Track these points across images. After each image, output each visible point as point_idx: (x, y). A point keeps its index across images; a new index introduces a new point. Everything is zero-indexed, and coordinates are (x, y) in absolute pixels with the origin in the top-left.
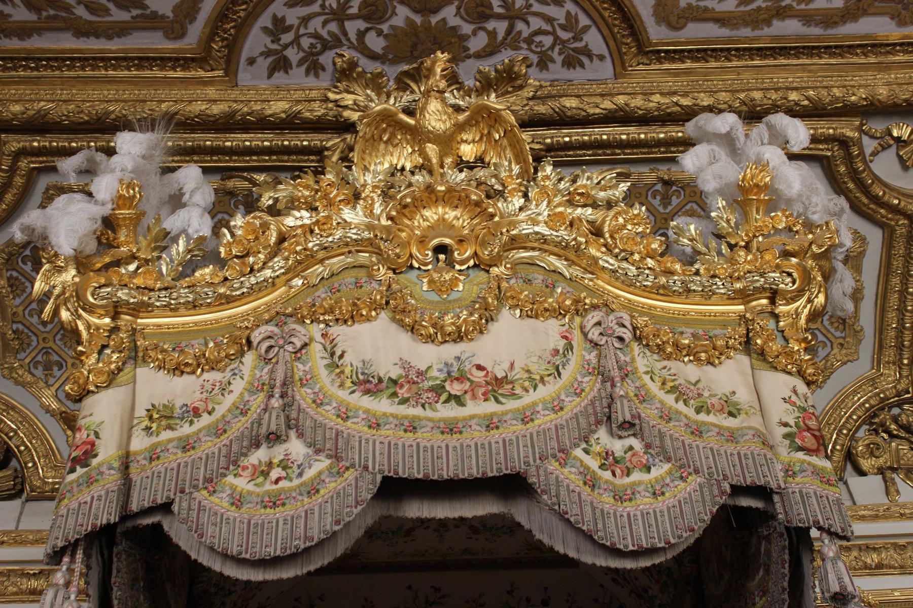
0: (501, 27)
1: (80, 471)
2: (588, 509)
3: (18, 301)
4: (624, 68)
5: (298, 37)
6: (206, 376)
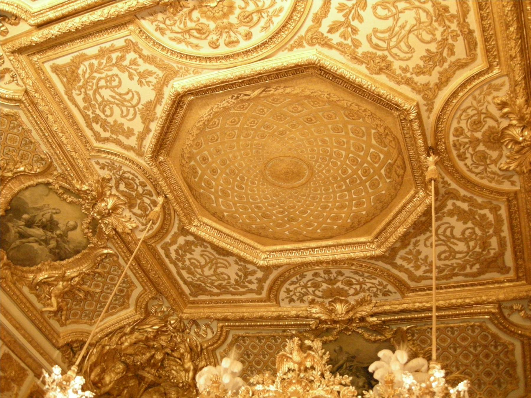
0: (358, 287)
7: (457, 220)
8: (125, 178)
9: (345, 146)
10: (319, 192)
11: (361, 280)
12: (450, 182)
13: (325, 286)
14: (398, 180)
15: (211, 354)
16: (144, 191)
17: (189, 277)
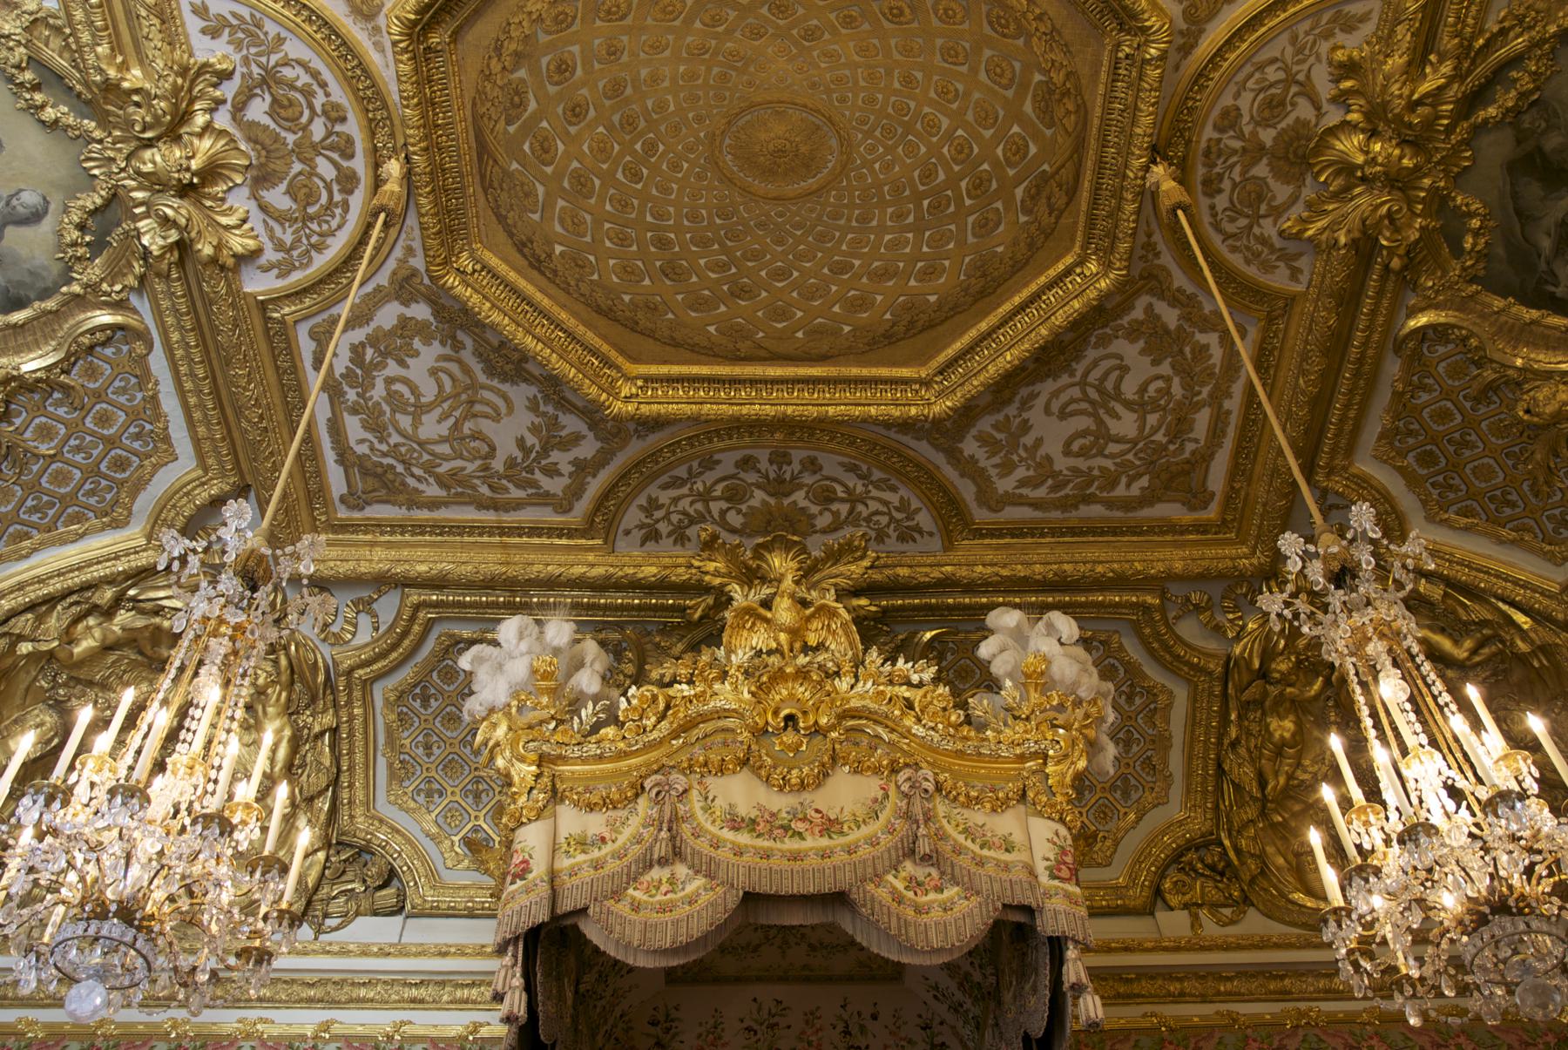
0: (844, 509)
1: (519, 883)
2: (894, 920)
3: (406, 734)
4: (951, 542)
5: (669, 513)
7: (1143, 352)
8: (279, 82)
9: (955, 106)
10: (842, 222)
11: (860, 489)
12: (1161, 247)
13: (759, 497)
14: (1047, 220)
15: (357, 694)
16: (329, 134)
17: (362, 441)
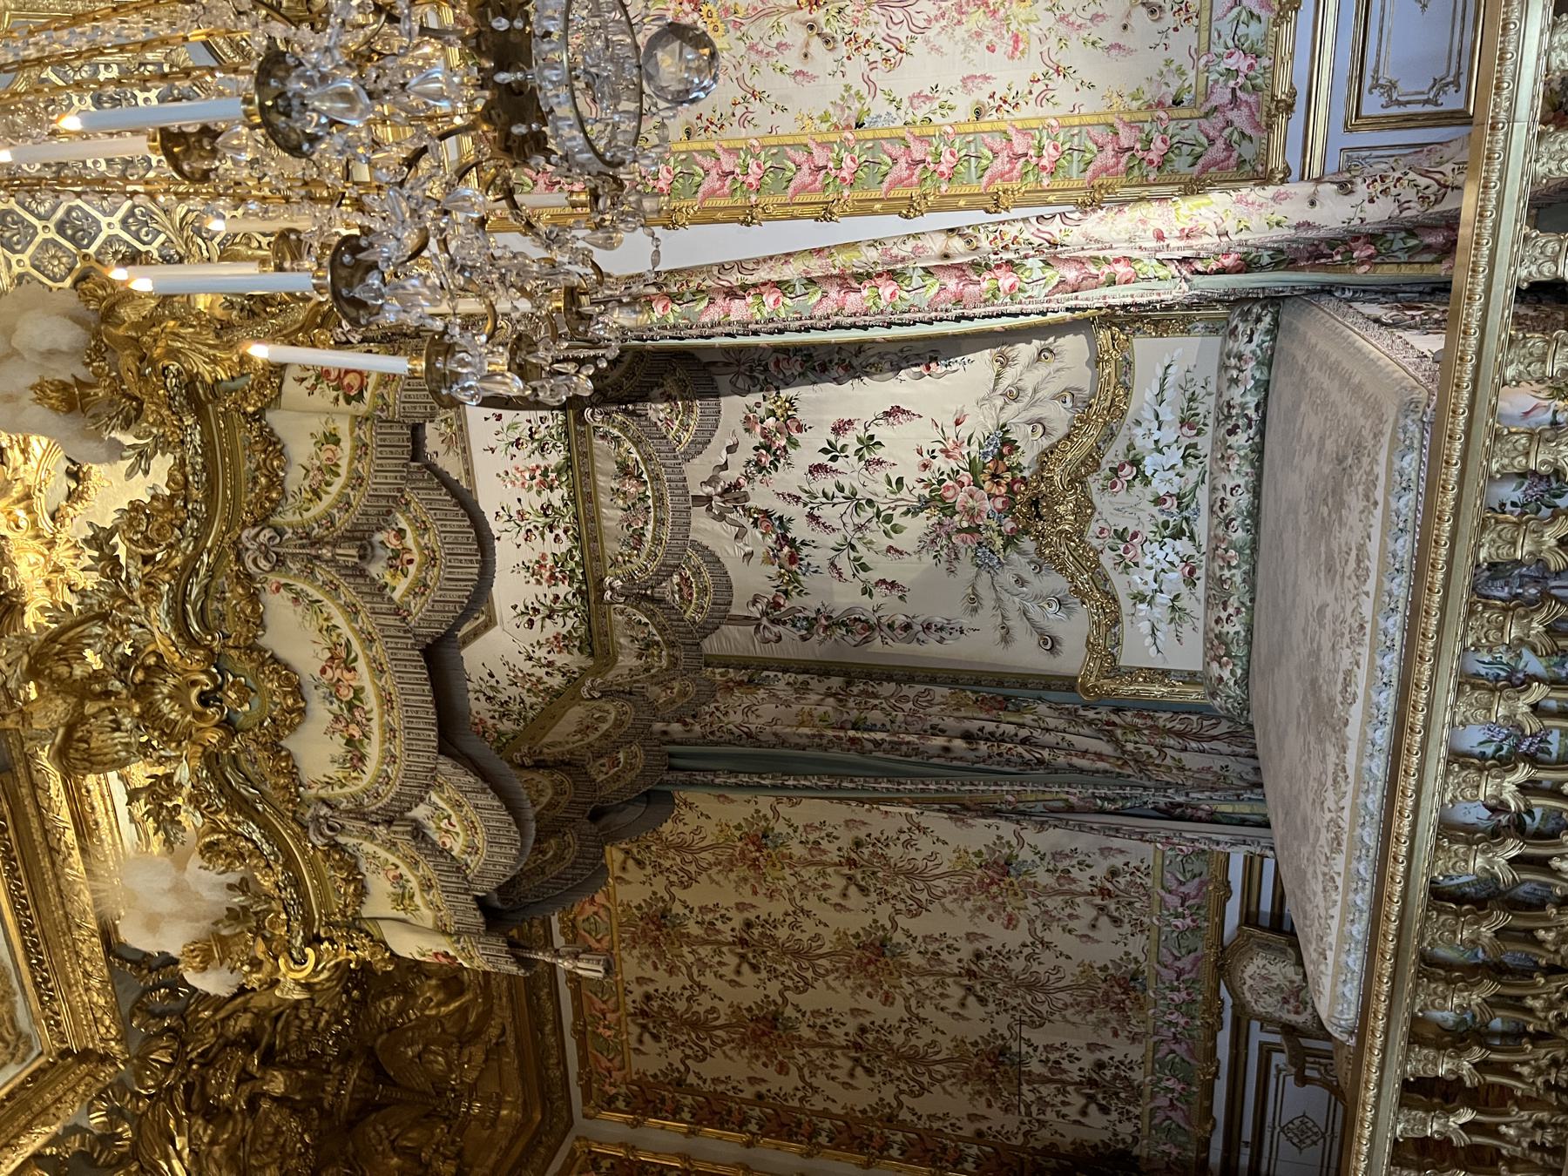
6: (363, 870)
